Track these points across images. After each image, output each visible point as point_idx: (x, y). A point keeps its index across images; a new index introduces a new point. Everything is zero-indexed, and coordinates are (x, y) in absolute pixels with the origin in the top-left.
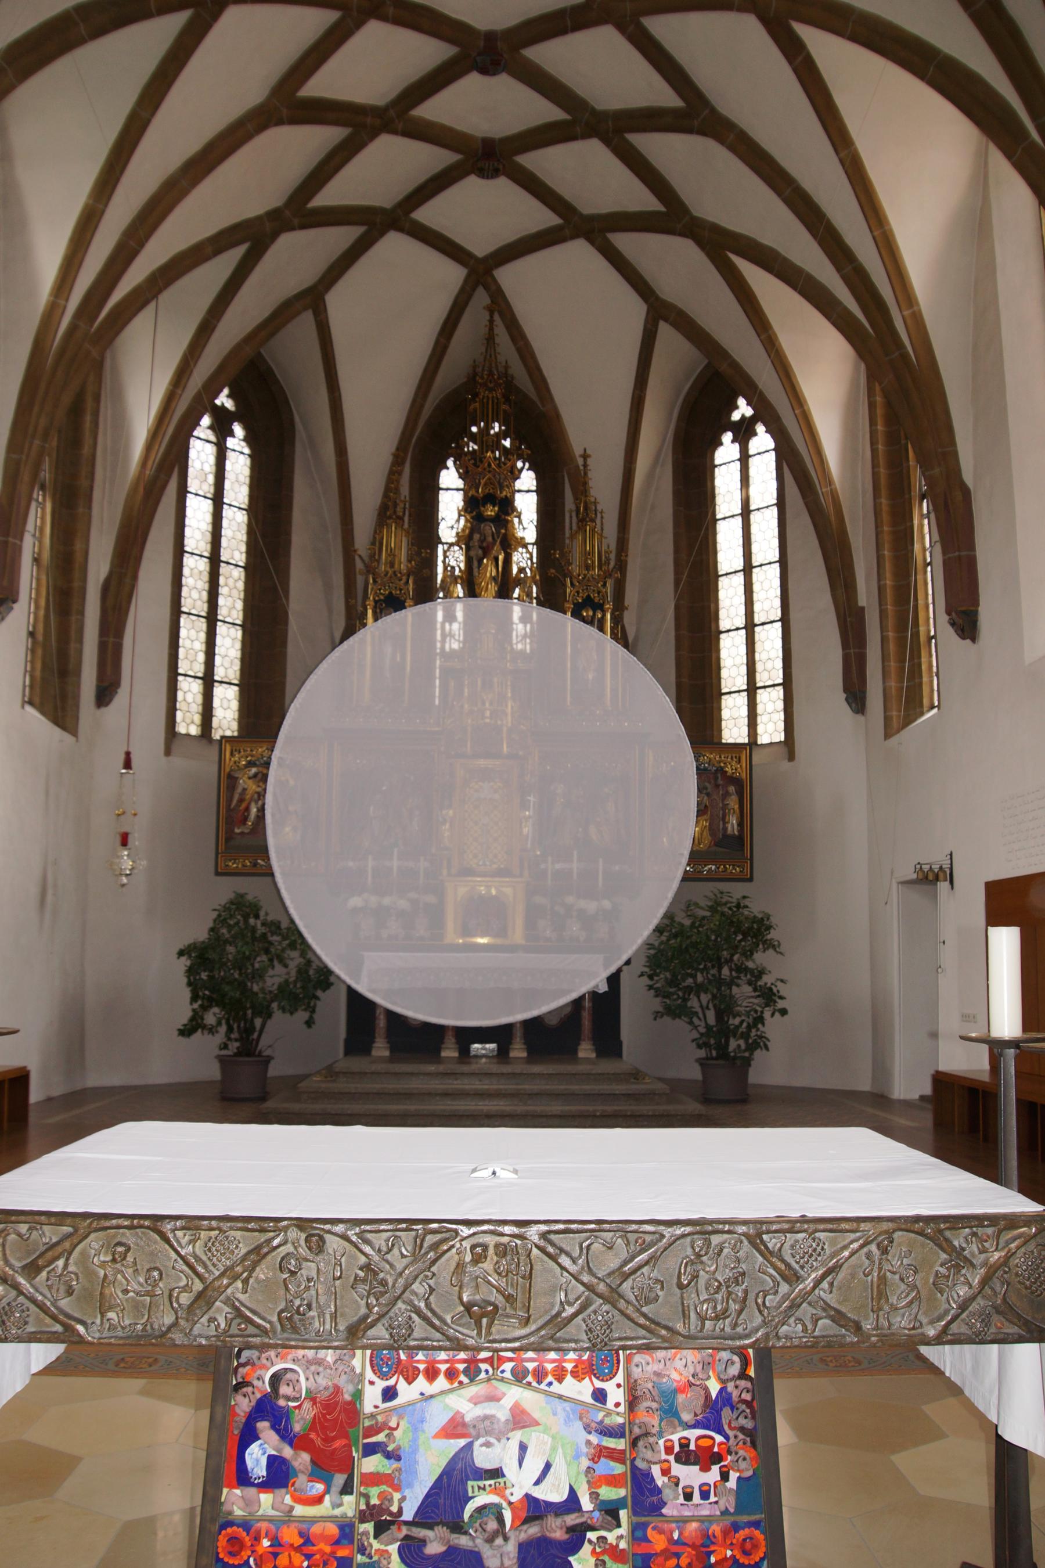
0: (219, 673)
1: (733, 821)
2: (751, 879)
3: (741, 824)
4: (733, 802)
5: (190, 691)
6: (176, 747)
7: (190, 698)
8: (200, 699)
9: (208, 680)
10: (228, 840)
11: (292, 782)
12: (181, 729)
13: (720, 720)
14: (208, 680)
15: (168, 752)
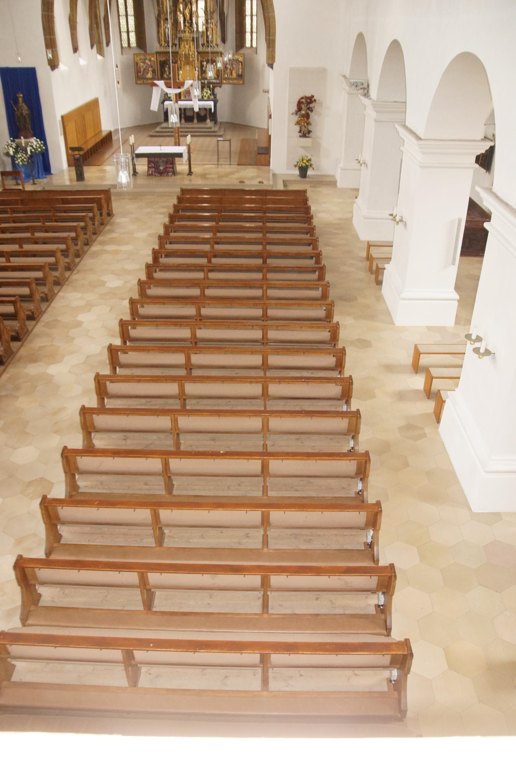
0: (130, 30)
1: (241, 71)
2: (244, 84)
3: (242, 72)
4: (240, 66)
5: (124, 36)
6: (124, 52)
7: (124, 38)
8: (127, 37)
9: (128, 32)
10: (138, 76)
11: (149, 63)
12: (124, 46)
13: (245, 39)
14: (128, 32)
15: (122, 54)
